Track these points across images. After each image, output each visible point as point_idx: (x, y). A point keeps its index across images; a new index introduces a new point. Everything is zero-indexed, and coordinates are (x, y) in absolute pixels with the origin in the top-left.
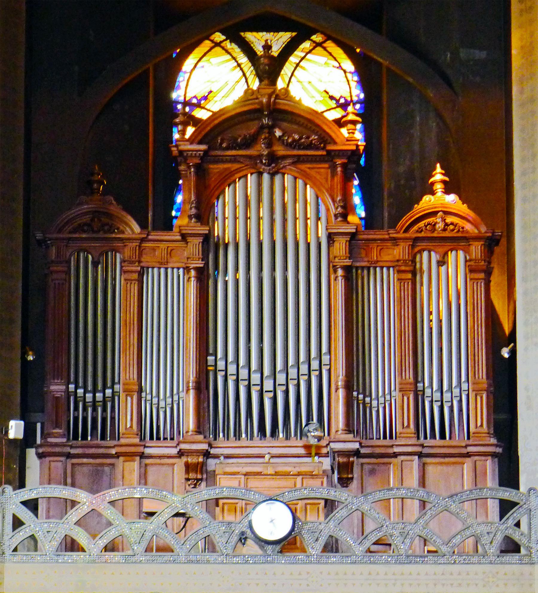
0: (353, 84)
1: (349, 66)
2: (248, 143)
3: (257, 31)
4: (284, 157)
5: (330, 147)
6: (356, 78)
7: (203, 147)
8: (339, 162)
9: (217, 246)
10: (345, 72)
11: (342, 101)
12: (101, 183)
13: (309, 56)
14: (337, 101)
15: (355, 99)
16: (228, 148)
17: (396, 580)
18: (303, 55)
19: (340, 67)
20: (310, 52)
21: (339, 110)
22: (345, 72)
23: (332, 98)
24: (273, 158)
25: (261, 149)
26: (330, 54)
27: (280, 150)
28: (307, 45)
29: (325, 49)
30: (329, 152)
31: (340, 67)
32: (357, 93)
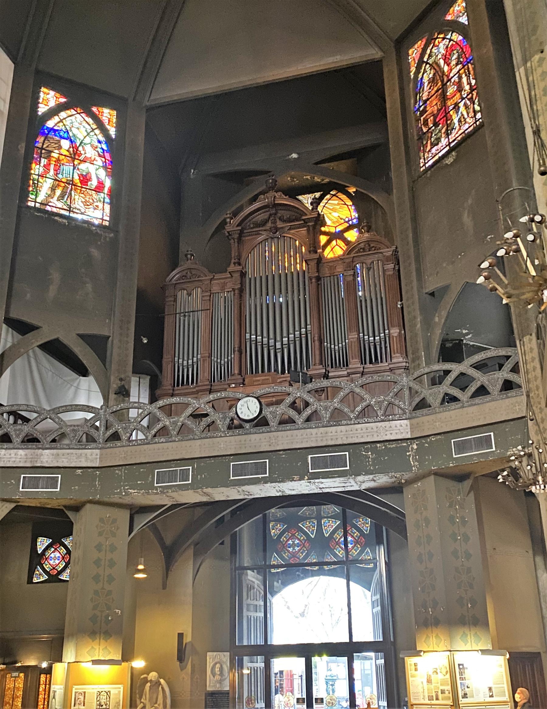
0: (352, 211)
1: (350, 203)
2: (264, 223)
3: (304, 194)
4: (282, 228)
5: (304, 218)
6: (353, 208)
7: (240, 228)
8: (310, 224)
9: (250, 279)
10: (347, 206)
11: (347, 220)
12: (192, 255)
13: (329, 202)
14: (344, 220)
15: (353, 217)
16: (253, 228)
17: (322, 437)
18: (326, 201)
19: (345, 204)
20: (330, 200)
21: (346, 223)
22: (347, 206)
23: (341, 219)
24: (277, 229)
25: (269, 225)
26: (340, 199)
27: (280, 224)
28: (328, 196)
29: (337, 197)
30: (304, 220)
31: (345, 204)
32: (355, 215)
